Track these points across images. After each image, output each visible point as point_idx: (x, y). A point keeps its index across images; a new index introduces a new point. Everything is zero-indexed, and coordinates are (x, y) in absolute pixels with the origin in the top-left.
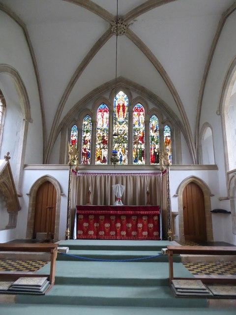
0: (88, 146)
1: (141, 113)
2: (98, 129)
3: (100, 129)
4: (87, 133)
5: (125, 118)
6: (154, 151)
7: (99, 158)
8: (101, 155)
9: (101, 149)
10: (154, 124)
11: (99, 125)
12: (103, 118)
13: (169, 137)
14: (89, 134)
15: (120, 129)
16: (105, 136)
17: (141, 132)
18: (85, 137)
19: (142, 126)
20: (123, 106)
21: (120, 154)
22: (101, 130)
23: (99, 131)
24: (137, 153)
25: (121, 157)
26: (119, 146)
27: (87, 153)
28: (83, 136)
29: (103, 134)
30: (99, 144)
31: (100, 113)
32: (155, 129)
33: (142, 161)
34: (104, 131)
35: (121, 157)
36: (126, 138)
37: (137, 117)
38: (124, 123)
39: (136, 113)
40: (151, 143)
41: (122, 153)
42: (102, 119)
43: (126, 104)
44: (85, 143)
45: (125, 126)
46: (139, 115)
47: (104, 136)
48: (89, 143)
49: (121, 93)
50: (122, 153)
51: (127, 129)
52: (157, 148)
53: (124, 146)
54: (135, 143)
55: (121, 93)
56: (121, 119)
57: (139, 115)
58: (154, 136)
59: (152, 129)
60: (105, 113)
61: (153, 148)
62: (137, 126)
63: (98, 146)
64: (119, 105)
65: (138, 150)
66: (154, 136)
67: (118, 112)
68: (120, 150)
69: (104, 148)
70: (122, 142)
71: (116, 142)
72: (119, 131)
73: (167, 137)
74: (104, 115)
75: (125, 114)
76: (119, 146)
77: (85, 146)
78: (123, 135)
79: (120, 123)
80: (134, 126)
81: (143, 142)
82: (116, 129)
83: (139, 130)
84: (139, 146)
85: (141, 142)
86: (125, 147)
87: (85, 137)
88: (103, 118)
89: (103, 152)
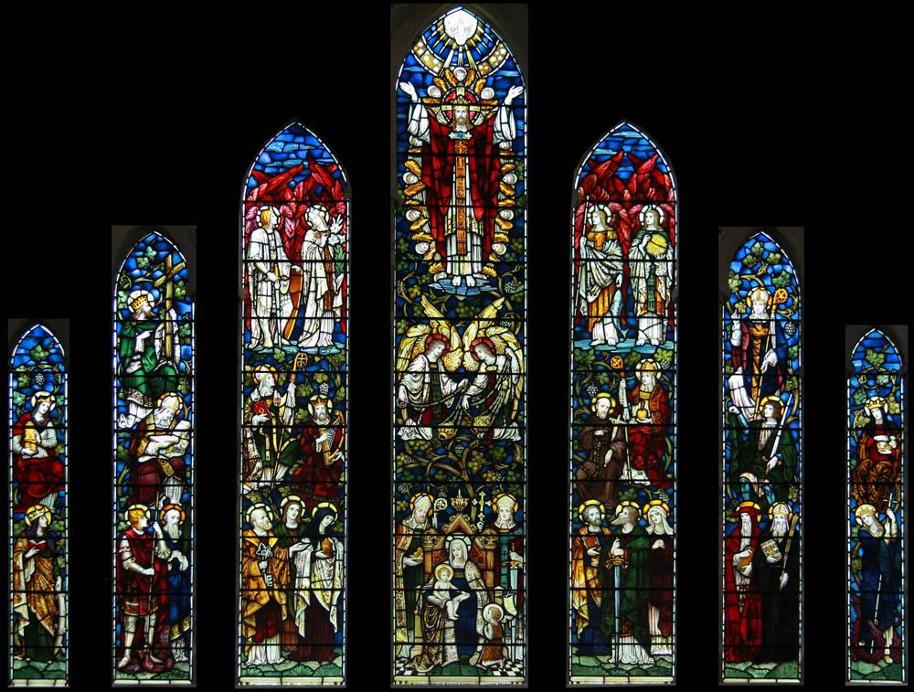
0: (173, 516)
1: (650, 217)
2: (256, 358)
3: (268, 359)
4: (152, 399)
5: (501, 265)
6: (758, 557)
7: (270, 623)
8: (290, 590)
9: (286, 539)
10: (758, 312)
11: (261, 333)
12: (295, 257)
13: (888, 428)
14: (171, 403)
15: (453, 362)
16: (322, 420)
17: (648, 382)
18: (141, 431)
19: (651, 330)
20: (483, 135)
21: (460, 582)
22: (282, 367)
23: (266, 380)
24: (605, 574)
25: (469, 609)
26: (444, 517)
27: (162, 573)
28: (127, 423)
29: (301, 402)
30: (271, 497)
31: (271, 215)
32: (771, 358)
33: (645, 642)
34: (305, 377)
35: (469, 609)
36: (509, 446)
37: (615, 249)
38: (490, 312)
39: (598, 218)
40: (735, 483)
41: (471, 572)
42: (285, 269)
43: (506, 127)
44: (146, 486)
45: (504, 337)
46: (626, 230)
47: (307, 429)
48: (174, 493)
49: (460, 24)
50: (471, 572)
51: (519, 361)
52: (780, 527)
53: (492, 517)
54: (591, 488)
55: (460, 24)
56: (466, 272)
57: (626, 230)
58: (756, 426)
59: (746, 358)
60: (316, 216)
61: (747, 528)
62: (605, 333)
63: (260, 518)
64: (439, 132)
65: (616, 550)
66: (756, 426)
67: (437, 204)
68: (459, 547)
69: (308, 529)
70: (477, 480)
71: (422, 482)
72: (449, 387)
73: (872, 429)
74: (304, 227)
75: (502, 228)
76: (444, 517)
77: (140, 517)
78: (480, 421)
79: (460, 311)
80: (586, 333)
81: (659, 479)
82: (419, 364)
83: (629, 370)
84: (624, 513)
85: (639, 476)
86: (504, 521)
87: (141, 431)
88: (295, 257)
89: (303, 565)
